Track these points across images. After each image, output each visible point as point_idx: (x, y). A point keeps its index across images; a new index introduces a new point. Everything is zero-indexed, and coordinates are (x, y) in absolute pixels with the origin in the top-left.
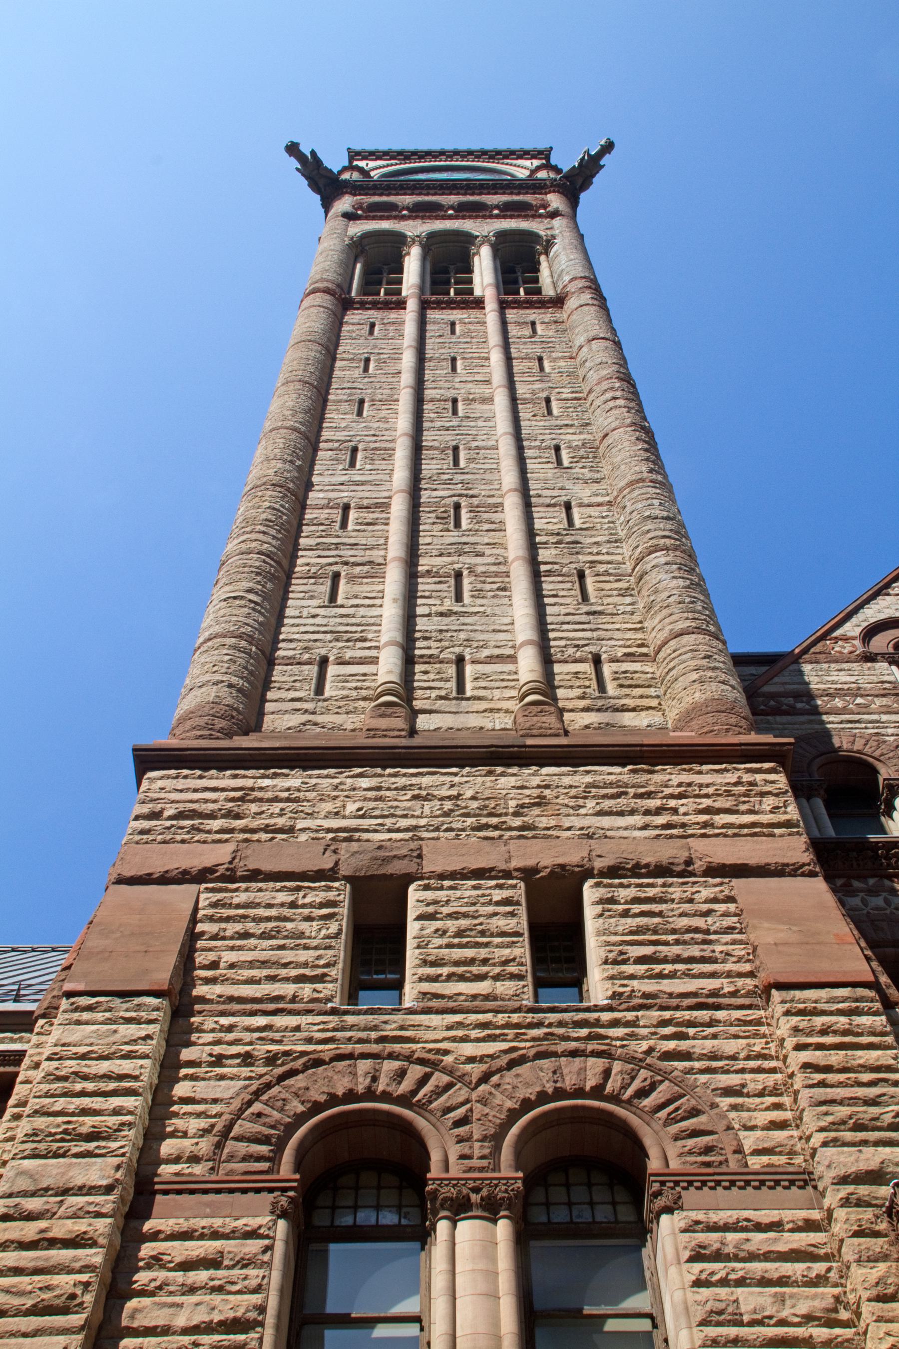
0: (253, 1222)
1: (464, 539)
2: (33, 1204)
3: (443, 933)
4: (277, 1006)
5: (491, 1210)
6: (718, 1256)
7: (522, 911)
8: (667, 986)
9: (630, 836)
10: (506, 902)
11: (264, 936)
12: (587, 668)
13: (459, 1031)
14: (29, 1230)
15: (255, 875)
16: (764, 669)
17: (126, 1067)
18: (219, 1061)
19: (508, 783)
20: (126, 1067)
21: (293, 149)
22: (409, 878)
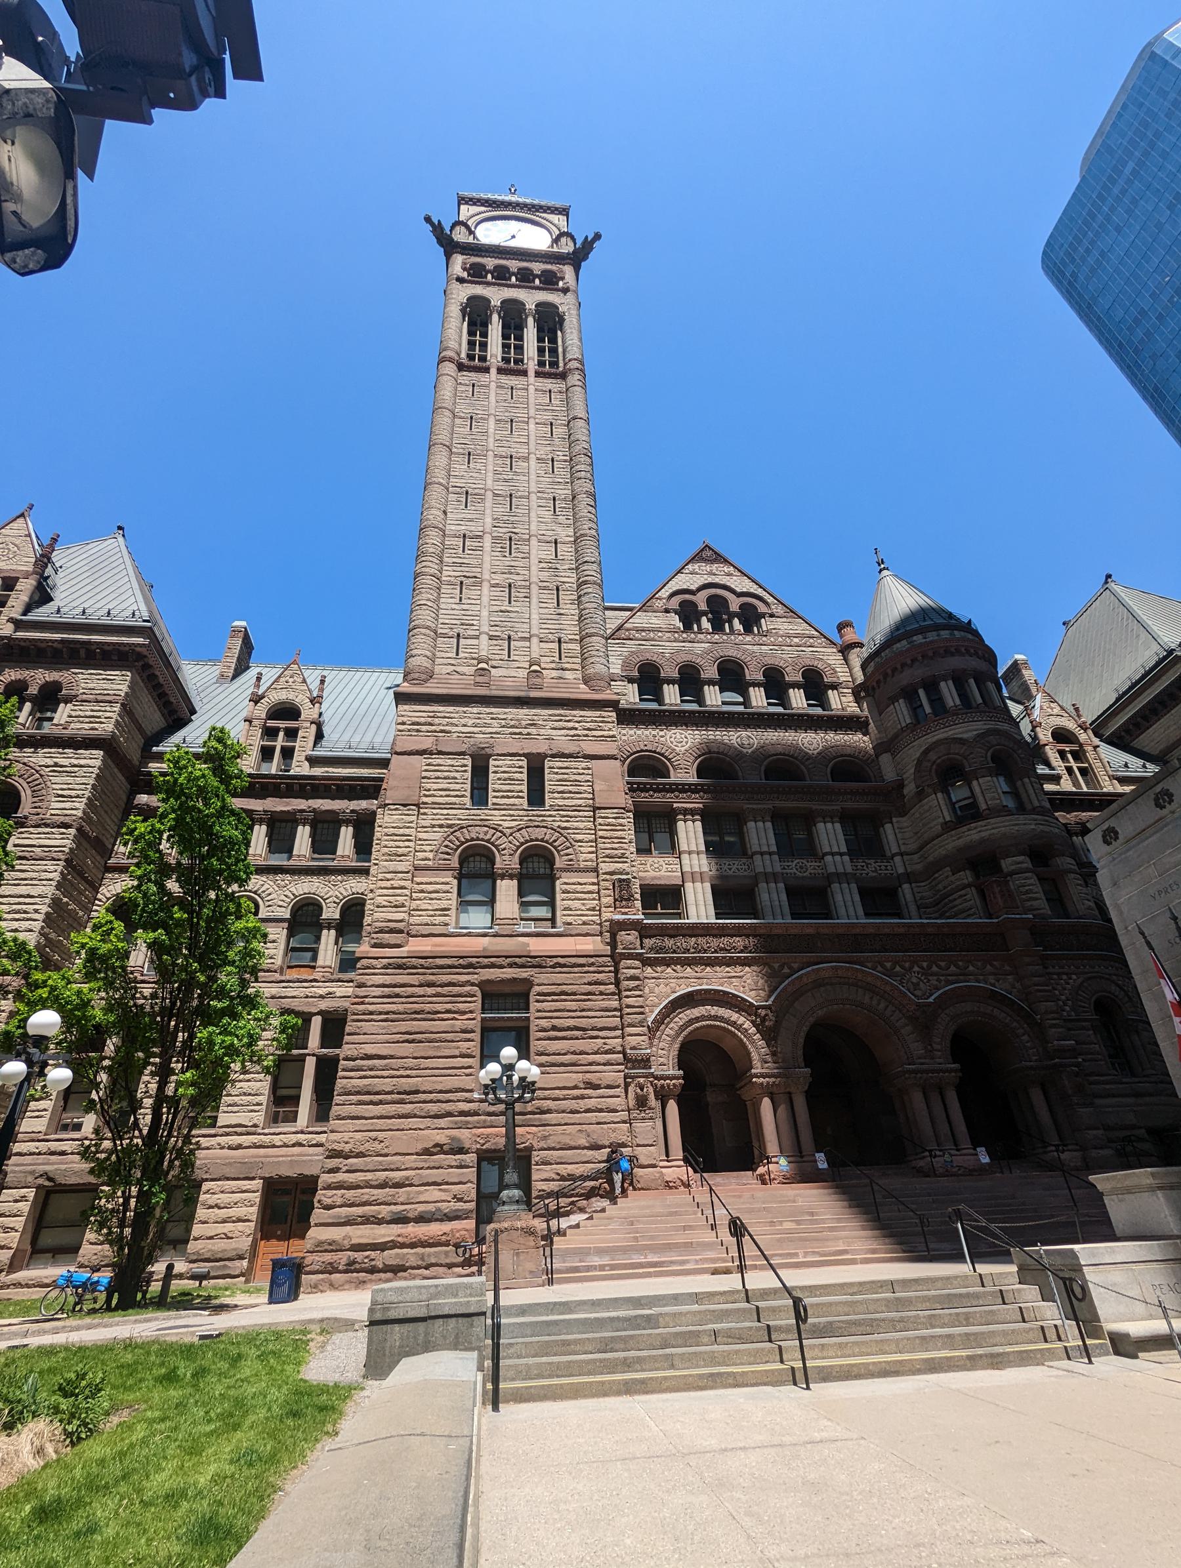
0: (448, 880)
1: (513, 564)
2: (389, 876)
3: (499, 779)
4: (452, 807)
5: (511, 877)
6: (569, 892)
7: (525, 771)
8: (567, 802)
9: (563, 742)
10: (520, 767)
11: (445, 778)
12: (557, 645)
13: (507, 819)
14: (388, 884)
15: (440, 753)
16: (628, 613)
17: (407, 831)
18: (433, 826)
19: (523, 713)
20: (407, 831)
21: (428, 219)
22: (491, 755)
